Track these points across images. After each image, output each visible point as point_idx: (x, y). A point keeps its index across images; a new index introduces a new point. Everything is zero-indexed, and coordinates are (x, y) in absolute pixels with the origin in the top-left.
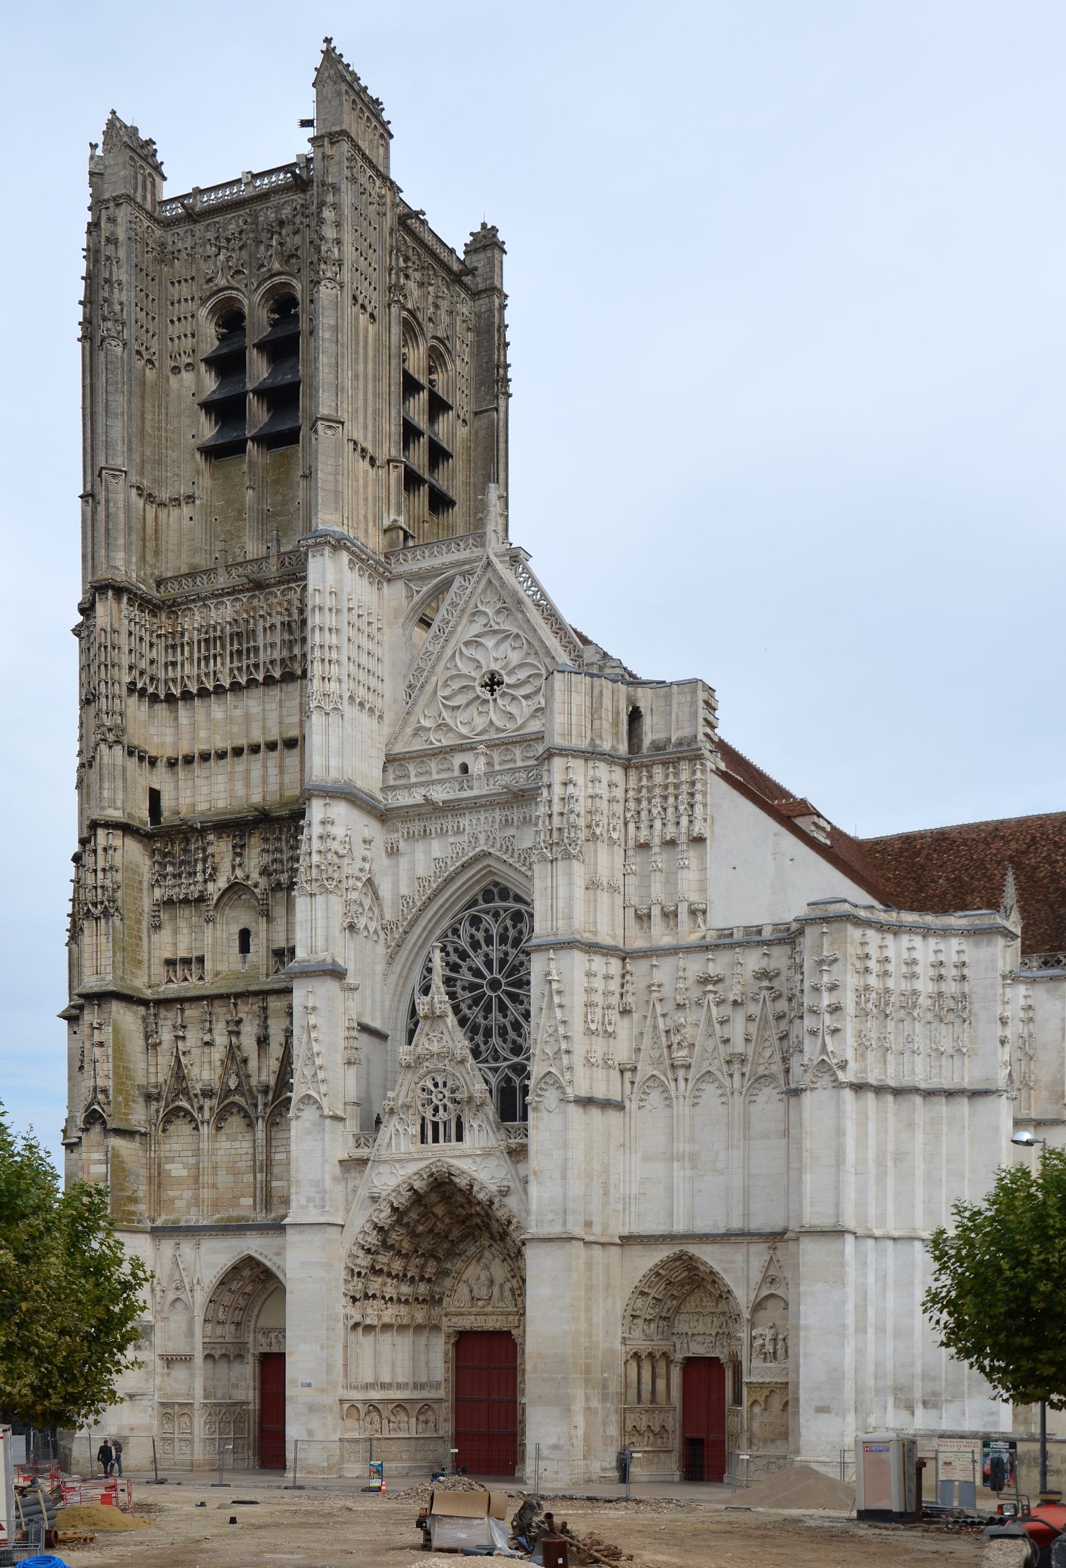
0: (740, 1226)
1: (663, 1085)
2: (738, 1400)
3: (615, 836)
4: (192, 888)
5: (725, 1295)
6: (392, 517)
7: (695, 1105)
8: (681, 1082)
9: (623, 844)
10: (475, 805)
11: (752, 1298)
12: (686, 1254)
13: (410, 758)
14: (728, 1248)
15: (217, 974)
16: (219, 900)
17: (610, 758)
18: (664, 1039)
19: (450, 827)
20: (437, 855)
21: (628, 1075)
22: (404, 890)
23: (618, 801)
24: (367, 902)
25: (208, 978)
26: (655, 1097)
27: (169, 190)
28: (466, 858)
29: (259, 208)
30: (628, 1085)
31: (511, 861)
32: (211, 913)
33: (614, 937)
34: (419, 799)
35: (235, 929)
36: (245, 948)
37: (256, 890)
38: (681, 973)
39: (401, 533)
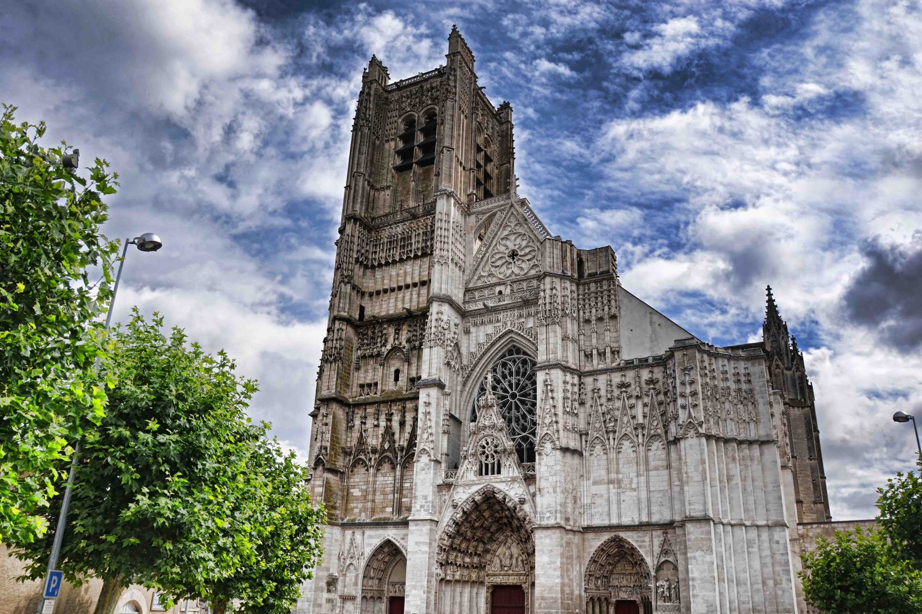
1: (602, 442)
3: (575, 315)
7: (619, 452)
8: (612, 440)
10: (506, 308)
11: (656, 563)
12: (617, 537)
14: (641, 534)
15: (383, 391)
17: (571, 279)
20: (489, 332)
21: (584, 437)
22: (473, 350)
24: (455, 354)
25: (379, 393)
26: (598, 447)
30: (584, 443)
33: (575, 364)
35: (393, 369)
36: (396, 379)
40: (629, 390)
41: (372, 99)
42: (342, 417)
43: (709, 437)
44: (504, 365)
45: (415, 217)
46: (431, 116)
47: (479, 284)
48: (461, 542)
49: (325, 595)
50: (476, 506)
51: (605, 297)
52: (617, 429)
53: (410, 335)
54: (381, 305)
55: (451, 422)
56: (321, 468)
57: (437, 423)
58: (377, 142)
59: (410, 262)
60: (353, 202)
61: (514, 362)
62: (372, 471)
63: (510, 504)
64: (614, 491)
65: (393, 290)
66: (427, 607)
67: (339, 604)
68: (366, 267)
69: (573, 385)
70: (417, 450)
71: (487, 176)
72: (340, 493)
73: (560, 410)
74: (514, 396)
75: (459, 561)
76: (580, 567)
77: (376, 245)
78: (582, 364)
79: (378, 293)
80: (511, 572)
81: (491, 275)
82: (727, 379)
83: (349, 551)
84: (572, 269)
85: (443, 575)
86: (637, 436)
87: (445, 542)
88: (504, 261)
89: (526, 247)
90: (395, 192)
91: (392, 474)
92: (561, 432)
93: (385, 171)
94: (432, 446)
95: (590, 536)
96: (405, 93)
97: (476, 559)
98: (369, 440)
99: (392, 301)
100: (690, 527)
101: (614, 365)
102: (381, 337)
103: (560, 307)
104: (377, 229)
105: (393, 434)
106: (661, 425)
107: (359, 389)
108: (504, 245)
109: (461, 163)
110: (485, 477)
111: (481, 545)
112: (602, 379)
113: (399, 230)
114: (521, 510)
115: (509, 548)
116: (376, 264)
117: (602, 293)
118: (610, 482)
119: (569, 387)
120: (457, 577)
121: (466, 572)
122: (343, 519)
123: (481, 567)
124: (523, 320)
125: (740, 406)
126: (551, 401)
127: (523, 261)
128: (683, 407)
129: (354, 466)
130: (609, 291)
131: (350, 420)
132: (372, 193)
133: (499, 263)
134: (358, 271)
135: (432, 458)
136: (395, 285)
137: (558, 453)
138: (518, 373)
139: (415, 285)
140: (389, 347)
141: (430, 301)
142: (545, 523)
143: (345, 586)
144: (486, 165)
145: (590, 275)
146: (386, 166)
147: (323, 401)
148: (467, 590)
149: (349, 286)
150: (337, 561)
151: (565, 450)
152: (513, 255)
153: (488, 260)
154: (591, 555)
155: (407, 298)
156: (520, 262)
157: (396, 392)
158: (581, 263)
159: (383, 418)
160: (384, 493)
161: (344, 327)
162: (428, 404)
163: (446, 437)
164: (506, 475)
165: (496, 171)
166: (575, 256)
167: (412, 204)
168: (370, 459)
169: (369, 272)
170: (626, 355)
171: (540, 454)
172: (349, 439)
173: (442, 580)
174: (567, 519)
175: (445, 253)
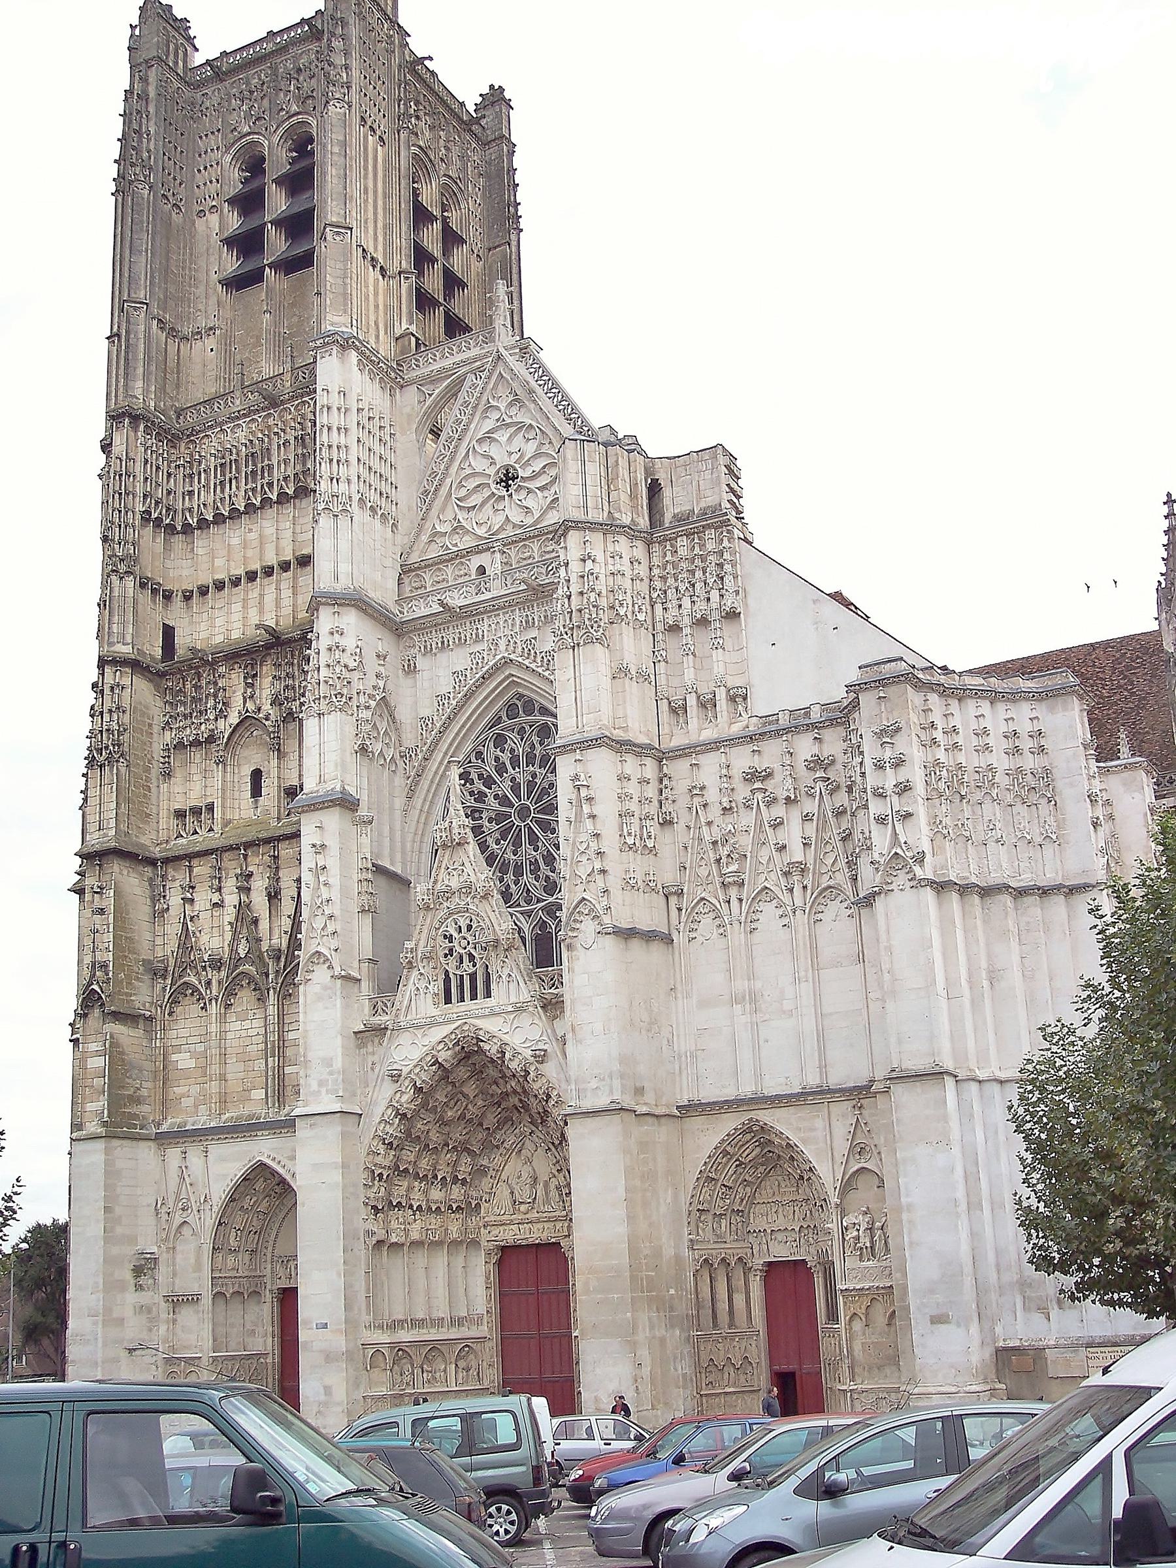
0: (818, 1081)
2: (833, 1316)
3: (641, 617)
4: (203, 727)
5: (806, 1176)
6: (404, 326)
8: (735, 903)
9: (650, 627)
13: (426, 566)
16: (229, 739)
17: (630, 532)
18: (711, 853)
19: (468, 636)
21: (673, 900)
22: (426, 712)
23: (642, 580)
24: (383, 726)
26: (707, 923)
27: (199, 59)
28: (487, 667)
29: (279, 61)
31: (533, 666)
32: (221, 753)
34: (437, 608)
35: (247, 770)
36: (256, 791)
37: (267, 723)
38: (724, 771)
39: (413, 339)
40: (770, 785)
41: (152, 109)
42: (138, 891)
43: (941, 887)
44: (500, 741)
45: (274, 402)
46: (303, 145)
47: (434, 552)
48: (418, 1157)
49: (132, 1298)
50: (444, 1073)
51: (712, 568)
52: (746, 877)
53: (280, 686)
54: (212, 619)
55: (382, 882)
56: (97, 1012)
57: (344, 891)
58: (177, 218)
59: (271, 512)
60: (126, 374)
61: (521, 732)
62: (213, 1009)
63: (513, 1065)
64: (743, 1019)
65: (236, 582)
66: (348, 1307)
67: (164, 1316)
68: (171, 529)
69: (644, 781)
70: (303, 955)
71: (452, 282)
72: (148, 1065)
73: (610, 843)
74: (523, 812)
75: (417, 1199)
76: (676, 1196)
77: (191, 476)
78: (665, 730)
79: (203, 591)
80: (534, 1215)
81: (458, 529)
82: (987, 747)
83: (178, 1194)
84: (634, 508)
85: (381, 1234)
86: (791, 890)
87: (379, 1160)
88: (486, 493)
89: (537, 455)
90: (227, 342)
91: (260, 1014)
92: (616, 894)
93: (202, 289)
94: (334, 943)
95: (696, 1123)
96: (232, 86)
97: (457, 1192)
98: (204, 939)
99: (237, 607)
100: (898, 1090)
101: (736, 729)
102: (215, 696)
103: (603, 602)
104: (191, 435)
105: (255, 922)
106: (842, 863)
107: (174, 822)
108: (486, 456)
109: (373, 259)
110: (456, 1008)
111: (466, 1159)
112: (710, 764)
113: (242, 435)
114: (539, 1075)
115: (529, 1161)
116: (193, 521)
117: (703, 559)
118: (736, 1000)
119: (633, 788)
120: (415, 1235)
121: (434, 1222)
122: (159, 1125)
123: (470, 1208)
124: (534, 633)
125: (1019, 808)
126: (589, 823)
127: (530, 491)
128: (881, 820)
129: (174, 1001)
130: (721, 553)
131: (157, 896)
132: (172, 348)
133: (475, 500)
134: (151, 542)
135: (337, 972)
136: (240, 571)
137: (609, 942)
138: (530, 760)
139: (285, 566)
140: (234, 719)
141: (314, 606)
142: (588, 1104)
143: (175, 1274)
144: (446, 252)
145: (680, 519)
146: (202, 276)
147: (92, 858)
148: (441, 1259)
149: (130, 582)
150: (152, 1220)
151: (627, 934)
152: (508, 478)
153: (449, 494)
154: (700, 1167)
155: (269, 599)
156: (523, 493)
157: (258, 822)
158: (654, 489)
159: (230, 884)
160: (246, 1060)
161: (126, 681)
162: (319, 849)
163: (368, 920)
164: (505, 1001)
165: (476, 266)
166: (641, 476)
167: (267, 368)
168: (209, 983)
169: (178, 541)
170: (763, 703)
171: (570, 947)
172: (159, 941)
173: (380, 1243)
174: (639, 1091)
175: (343, 487)
